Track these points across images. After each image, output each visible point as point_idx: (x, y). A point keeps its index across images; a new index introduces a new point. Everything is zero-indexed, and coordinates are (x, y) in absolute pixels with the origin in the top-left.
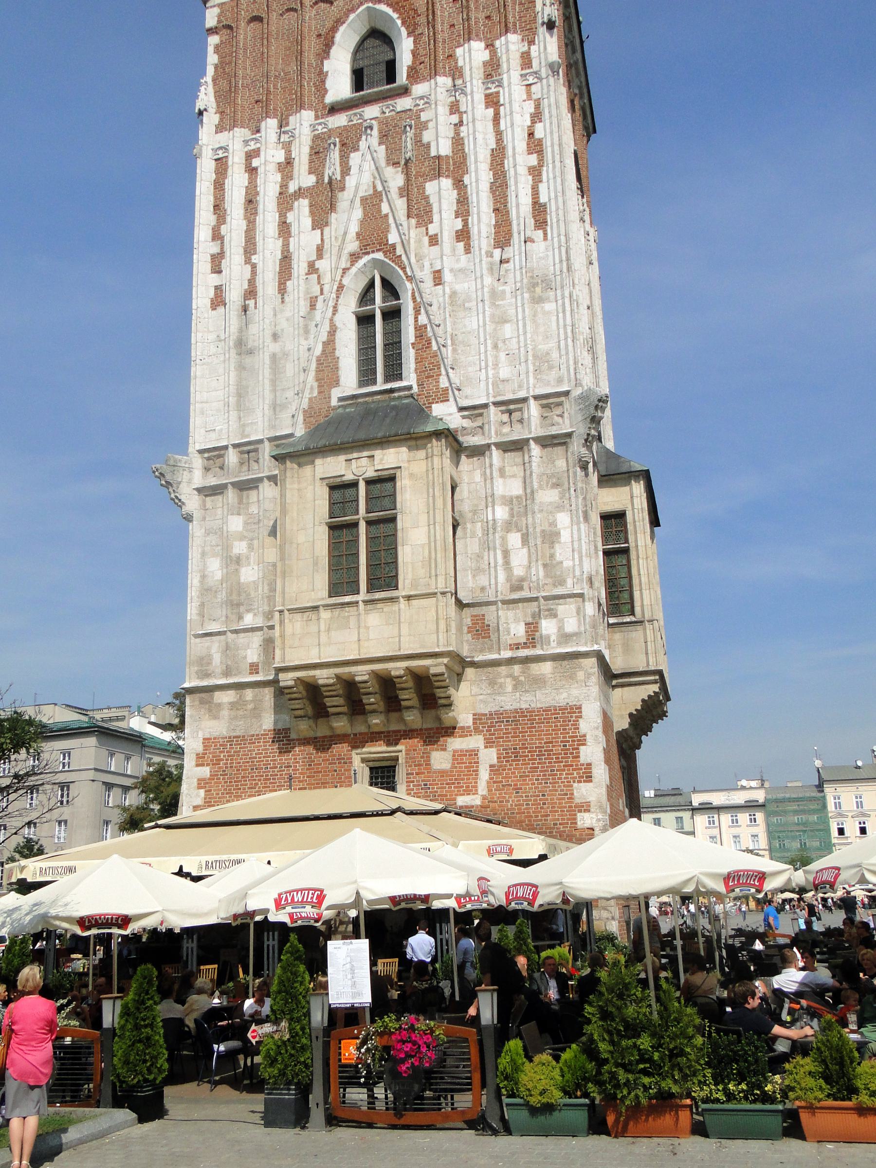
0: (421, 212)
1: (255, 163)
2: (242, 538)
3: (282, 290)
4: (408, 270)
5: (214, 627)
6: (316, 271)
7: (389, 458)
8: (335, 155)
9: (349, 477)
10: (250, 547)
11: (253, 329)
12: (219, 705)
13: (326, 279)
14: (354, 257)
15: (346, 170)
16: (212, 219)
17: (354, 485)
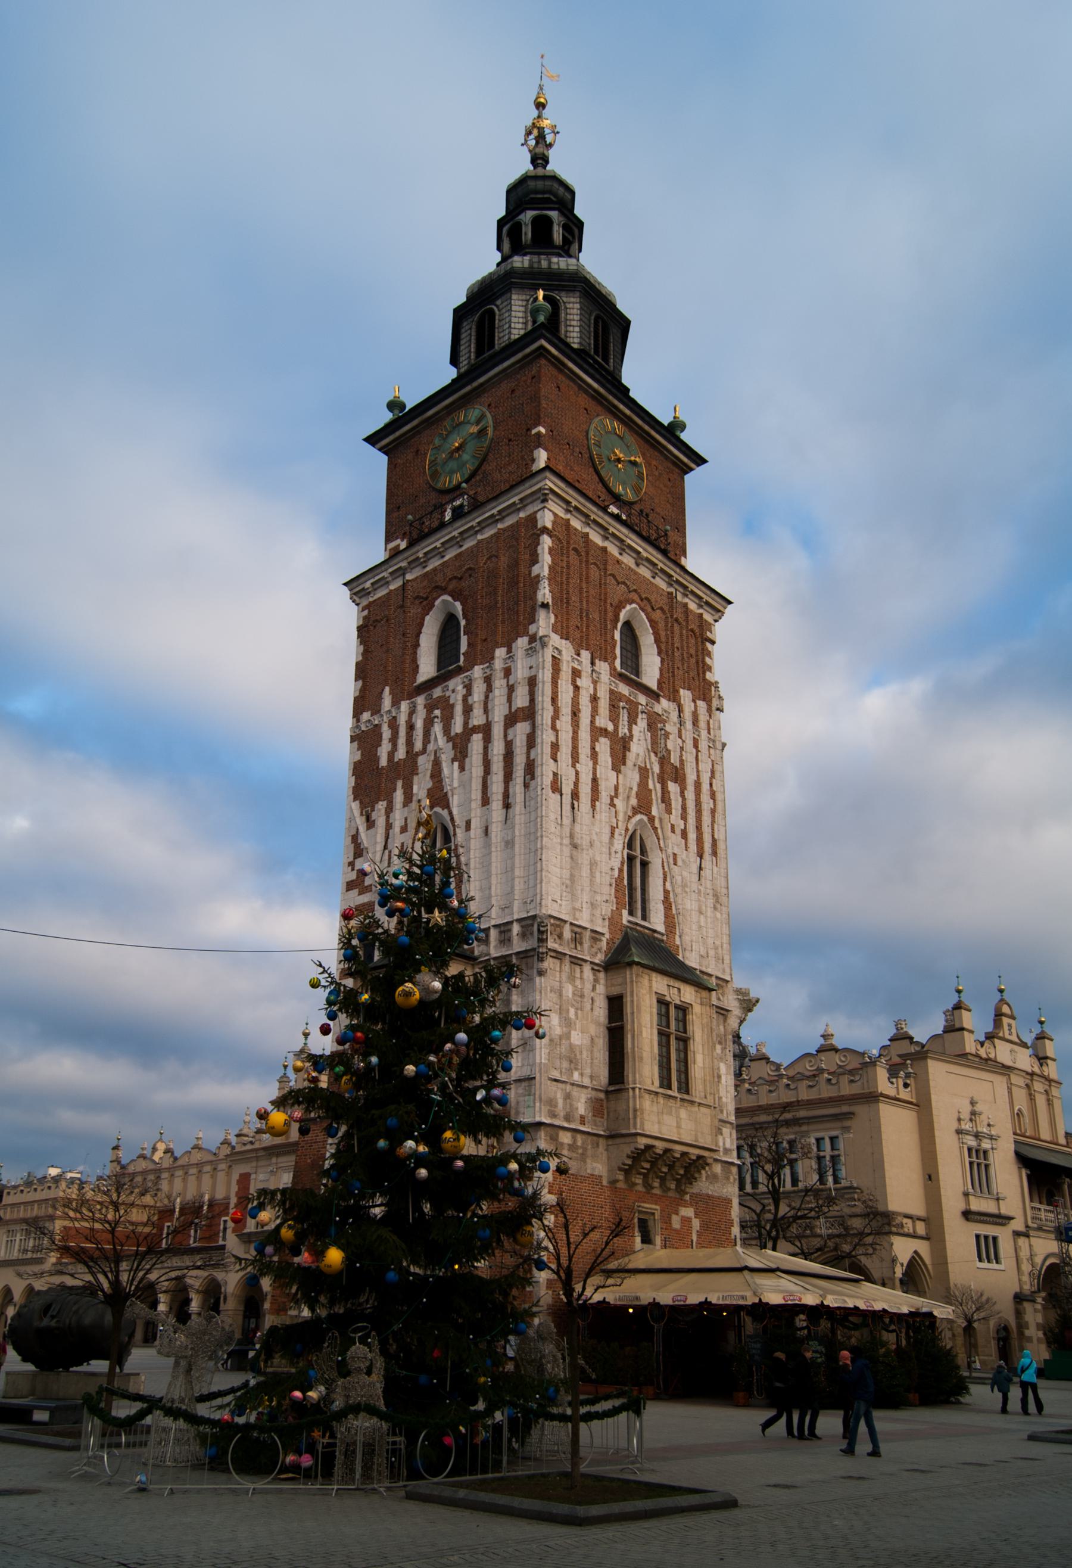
0: (665, 799)
1: (579, 682)
2: (573, 1006)
3: (593, 806)
4: (661, 842)
5: (556, 1074)
6: (614, 806)
7: (688, 994)
8: (624, 717)
9: (668, 999)
10: (576, 1014)
11: (577, 828)
12: (562, 1144)
13: (621, 817)
14: (636, 811)
15: (631, 737)
16: (551, 708)
17: (667, 1004)
